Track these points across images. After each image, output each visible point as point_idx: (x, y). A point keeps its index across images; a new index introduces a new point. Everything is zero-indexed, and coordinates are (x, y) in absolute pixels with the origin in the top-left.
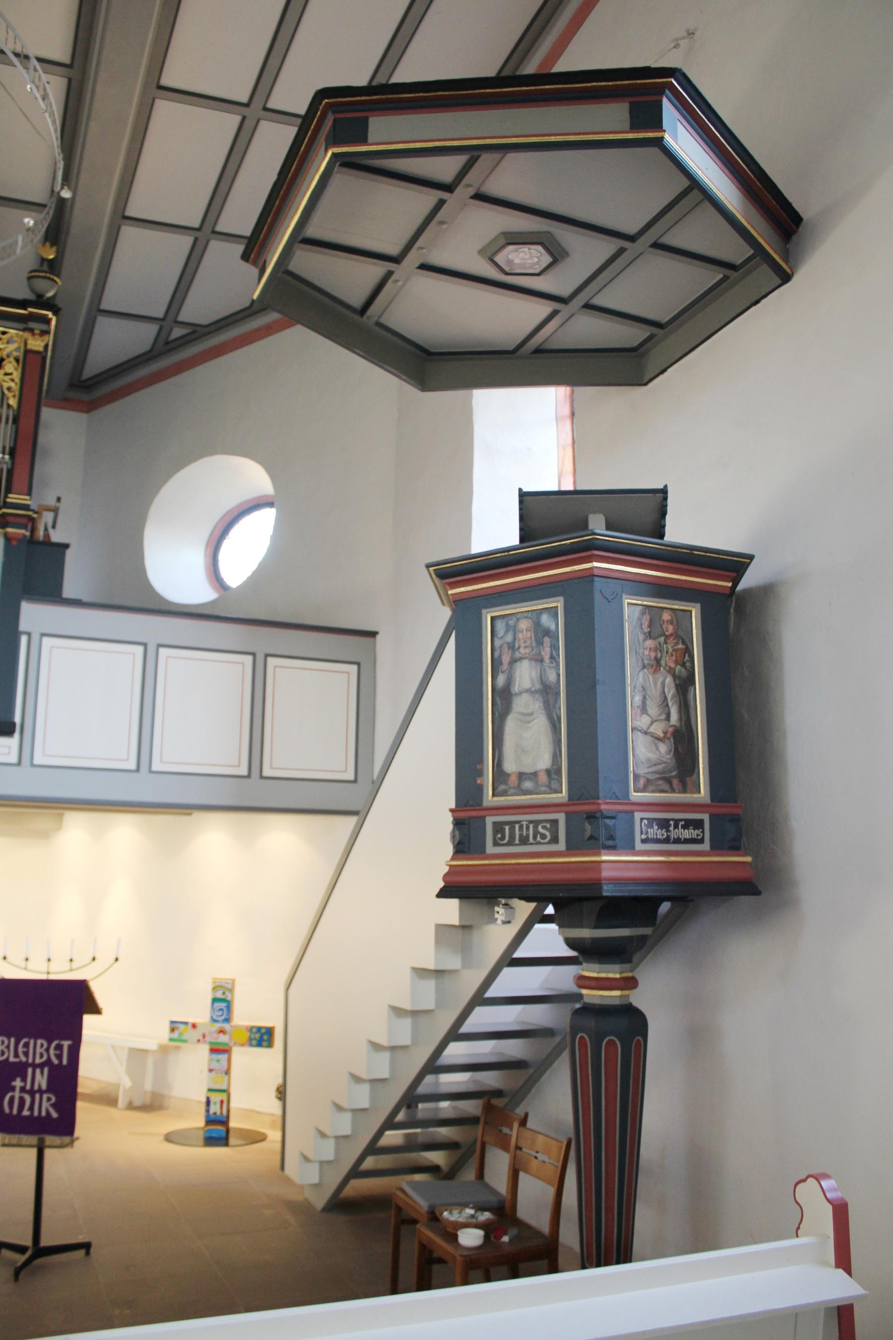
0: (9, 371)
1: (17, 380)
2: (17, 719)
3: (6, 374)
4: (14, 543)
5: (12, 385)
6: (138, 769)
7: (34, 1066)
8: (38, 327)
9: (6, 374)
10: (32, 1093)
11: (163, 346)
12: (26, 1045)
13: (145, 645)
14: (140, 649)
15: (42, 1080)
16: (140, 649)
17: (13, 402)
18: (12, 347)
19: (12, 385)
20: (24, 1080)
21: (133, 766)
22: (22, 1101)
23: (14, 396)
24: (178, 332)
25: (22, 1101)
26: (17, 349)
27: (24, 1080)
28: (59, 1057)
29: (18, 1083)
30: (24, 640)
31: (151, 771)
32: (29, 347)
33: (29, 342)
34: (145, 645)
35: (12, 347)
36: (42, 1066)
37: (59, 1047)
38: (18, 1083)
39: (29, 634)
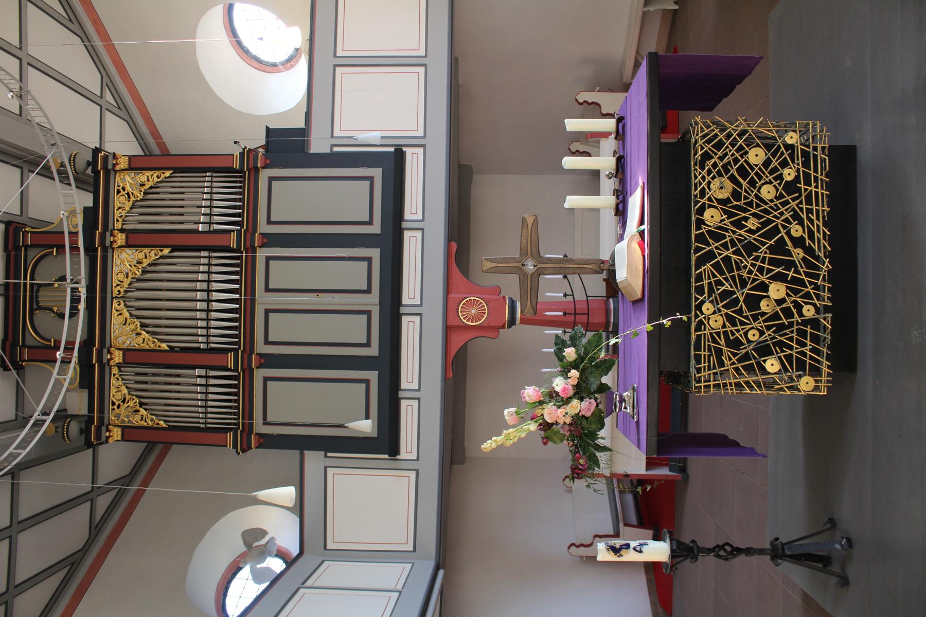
0: (146, 179)
1: (152, 173)
2: (392, 149)
5: (155, 175)
6: (425, 65)
11: (121, 109)
13: (335, 66)
14: (339, 70)
16: (339, 70)
17: (168, 173)
18: (128, 178)
19: (155, 175)
24: (109, 97)
30: (336, 149)
32: (126, 166)
33: (122, 167)
34: (335, 66)
39: (333, 146)
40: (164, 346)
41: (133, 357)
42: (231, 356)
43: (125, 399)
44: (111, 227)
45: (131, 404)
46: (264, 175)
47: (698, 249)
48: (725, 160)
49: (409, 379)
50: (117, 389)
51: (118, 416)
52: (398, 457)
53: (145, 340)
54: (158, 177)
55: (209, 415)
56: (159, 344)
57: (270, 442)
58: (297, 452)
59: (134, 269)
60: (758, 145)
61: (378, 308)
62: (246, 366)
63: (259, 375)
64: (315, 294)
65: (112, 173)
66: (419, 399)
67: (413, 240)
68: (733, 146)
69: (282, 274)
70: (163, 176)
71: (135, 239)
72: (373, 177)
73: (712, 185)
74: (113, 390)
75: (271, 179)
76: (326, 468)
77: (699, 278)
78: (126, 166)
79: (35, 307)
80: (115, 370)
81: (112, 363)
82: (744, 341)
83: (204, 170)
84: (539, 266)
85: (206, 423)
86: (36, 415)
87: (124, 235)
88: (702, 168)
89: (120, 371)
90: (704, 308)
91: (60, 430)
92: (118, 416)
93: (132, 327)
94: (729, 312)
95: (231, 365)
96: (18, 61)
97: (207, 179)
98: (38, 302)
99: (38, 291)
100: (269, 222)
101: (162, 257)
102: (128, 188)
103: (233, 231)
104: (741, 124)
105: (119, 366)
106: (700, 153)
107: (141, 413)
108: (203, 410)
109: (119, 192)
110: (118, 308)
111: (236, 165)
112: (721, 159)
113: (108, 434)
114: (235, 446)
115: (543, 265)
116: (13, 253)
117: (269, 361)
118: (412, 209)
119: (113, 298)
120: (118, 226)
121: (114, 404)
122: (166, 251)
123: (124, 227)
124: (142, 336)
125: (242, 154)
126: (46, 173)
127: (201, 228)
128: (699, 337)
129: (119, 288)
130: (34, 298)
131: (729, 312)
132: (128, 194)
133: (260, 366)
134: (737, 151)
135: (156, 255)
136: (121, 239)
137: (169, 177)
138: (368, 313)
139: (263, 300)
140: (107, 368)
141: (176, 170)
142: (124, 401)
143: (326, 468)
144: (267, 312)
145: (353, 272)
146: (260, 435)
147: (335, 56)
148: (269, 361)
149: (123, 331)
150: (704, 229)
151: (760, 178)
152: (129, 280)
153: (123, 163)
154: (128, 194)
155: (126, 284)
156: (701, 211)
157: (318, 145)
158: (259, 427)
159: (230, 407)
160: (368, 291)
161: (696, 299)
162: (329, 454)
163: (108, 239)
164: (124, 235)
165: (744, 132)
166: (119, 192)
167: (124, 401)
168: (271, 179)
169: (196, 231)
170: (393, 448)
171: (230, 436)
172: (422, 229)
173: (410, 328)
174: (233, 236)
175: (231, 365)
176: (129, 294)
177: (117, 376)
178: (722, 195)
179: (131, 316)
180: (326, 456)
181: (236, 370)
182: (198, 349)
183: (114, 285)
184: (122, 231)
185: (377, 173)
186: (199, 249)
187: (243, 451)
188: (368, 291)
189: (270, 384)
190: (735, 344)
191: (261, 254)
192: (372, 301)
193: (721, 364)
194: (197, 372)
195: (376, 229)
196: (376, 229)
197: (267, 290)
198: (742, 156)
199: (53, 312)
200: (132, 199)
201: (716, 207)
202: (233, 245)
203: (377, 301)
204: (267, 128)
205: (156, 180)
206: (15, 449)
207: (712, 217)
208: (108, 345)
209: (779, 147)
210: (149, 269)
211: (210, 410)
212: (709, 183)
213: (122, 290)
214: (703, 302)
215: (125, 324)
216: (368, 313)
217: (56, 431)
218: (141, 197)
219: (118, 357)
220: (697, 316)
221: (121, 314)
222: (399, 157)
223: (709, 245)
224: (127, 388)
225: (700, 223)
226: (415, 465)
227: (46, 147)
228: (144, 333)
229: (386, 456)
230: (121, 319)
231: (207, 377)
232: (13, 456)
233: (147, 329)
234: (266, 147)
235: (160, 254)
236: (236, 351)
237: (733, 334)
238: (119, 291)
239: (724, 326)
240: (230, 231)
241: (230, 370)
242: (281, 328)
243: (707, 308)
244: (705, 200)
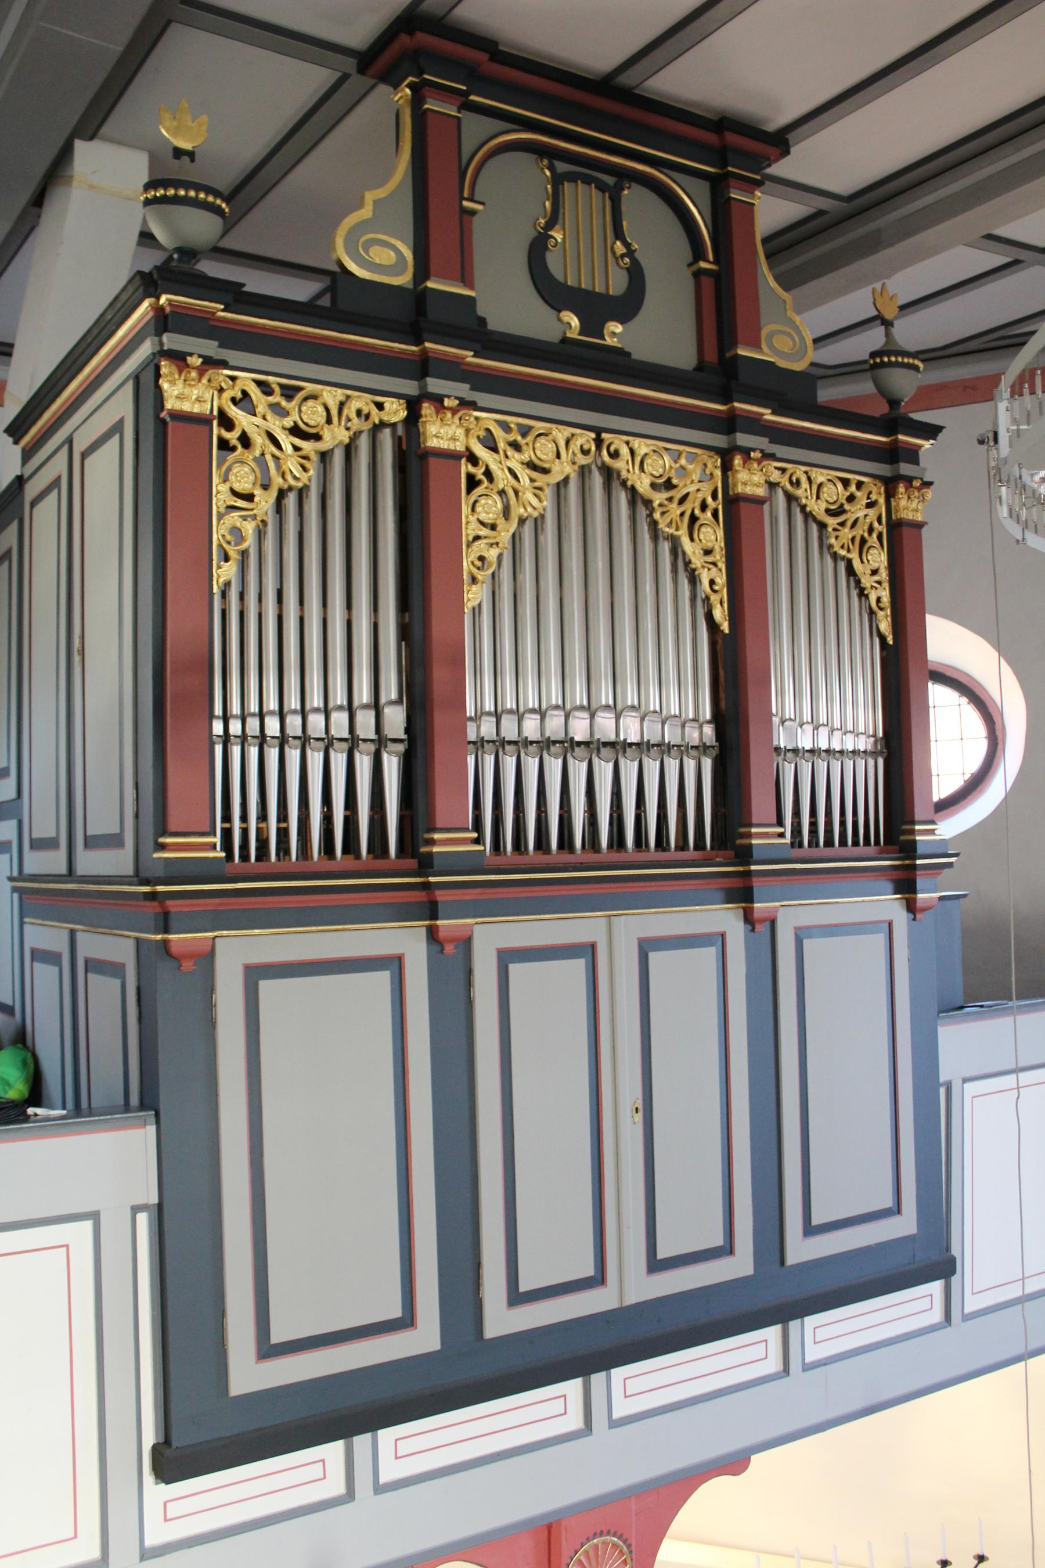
52: (148, 1477)
61: (614, 1304)
66: (350, 1494)
69: (686, 986)
79: (562, 167)
98: (572, 177)
99: (602, 187)
113: (196, 361)
116: (710, 138)
117: (452, 966)
119: (598, 431)
124: (501, 523)
144: (589, 951)
148: (452, 966)
159: (263, 817)
162: (143, 1218)
177: (376, 416)
180: (135, 1210)
183: (636, 442)
189: (383, 978)
199: (551, 224)
200: (832, 522)
203: (632, 1298)
211: (272, 755)
231: (381, 741)
242: (548, 997)
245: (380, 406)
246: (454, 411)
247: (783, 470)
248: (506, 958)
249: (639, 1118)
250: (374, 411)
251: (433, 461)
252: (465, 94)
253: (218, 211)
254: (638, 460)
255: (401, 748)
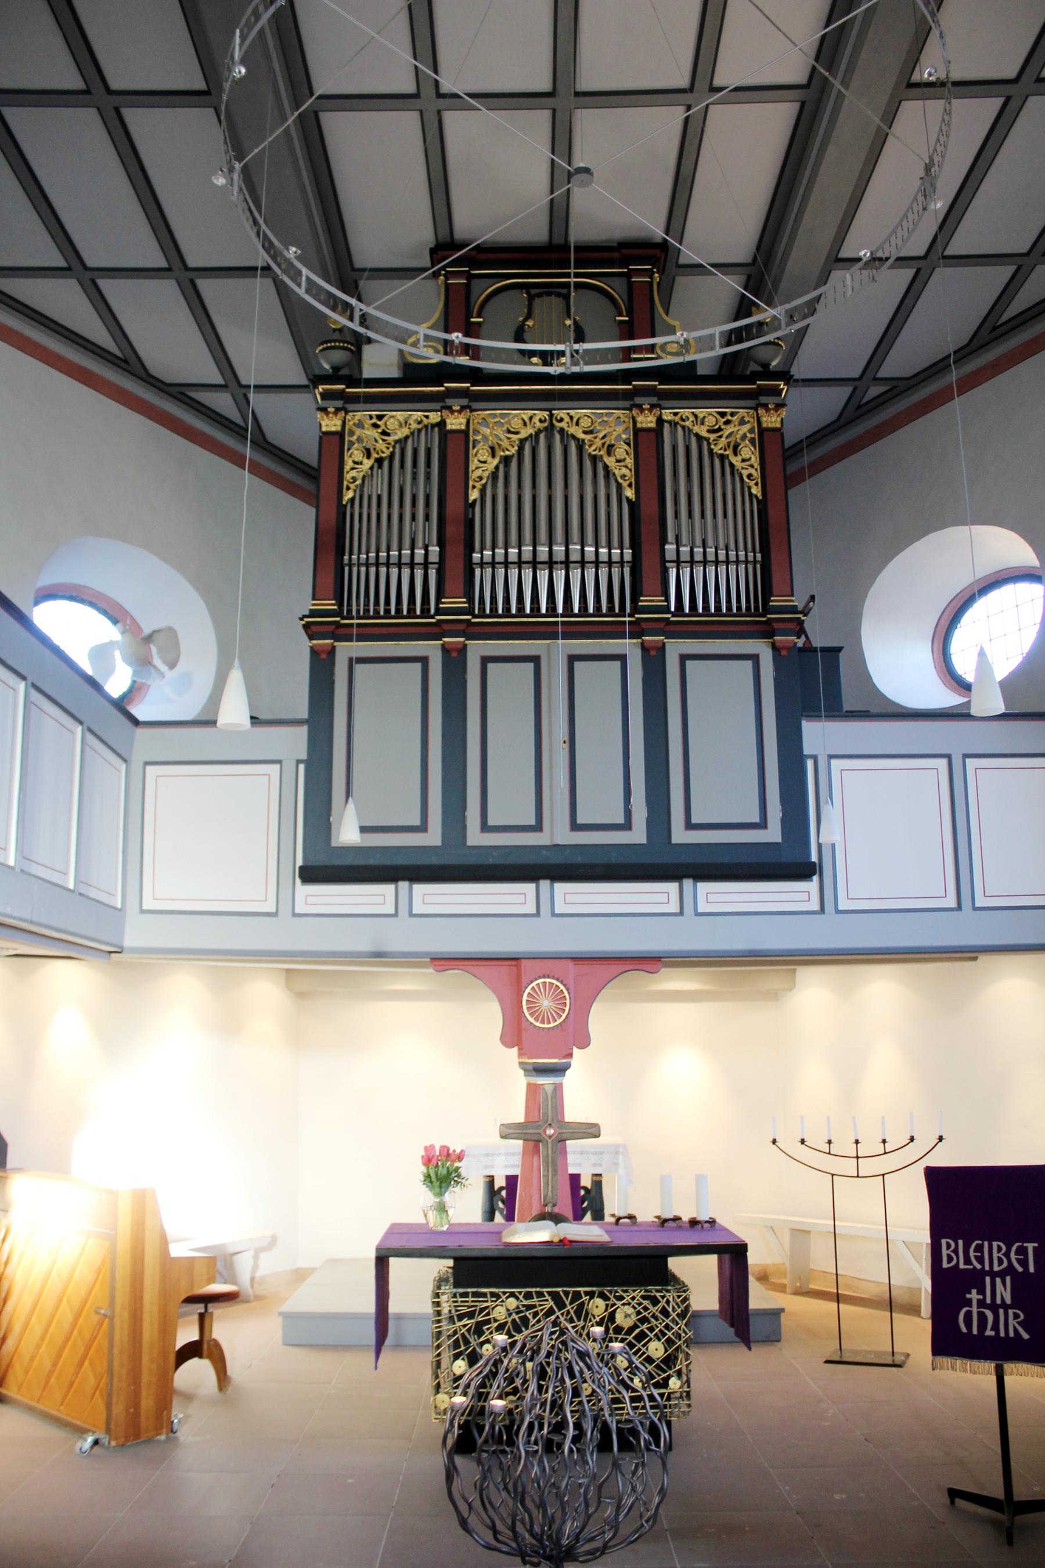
0: (748, 456)
1: (756, 465)
2: (814, 858)
3: (743, 461)
4: (784, 653)
5: (753, 471)
6: (959, 907)
7: (993, 1275)
8: (771, 401)
9: (743, 461)
10: (994, 1308)
12: (979, 1249)
13: (949, 757)
14: (943, 763)
15: (1004, 1292)
16: (943, 763)
18: (745, 428)
19: (753, 471)
20: (982, 1291)
21: (953, 904)
22: (982, 1318)
23: (756, 484)
25: (982, 1318)
26: (751, 431)
27: (982, 1291)
28: (1024, 1263)
29: (974, 1295)
30: (810, 764)
31: (975, 909)
32: (765, 425)
33: (764, 419)
34: (949, 757)
35: (747, 427)
36: (1002, 1274)
37: (1021, 1251)
38: (974, 1295)
40: (474, 495)
41: (454, 447)
42: (461, 603)
43: (388, 435)
44: (664, 403)
45: (381, 445)
46: (761, 648)
47: (567, 1293)
48: (652, 1320)
49: (430, 896)
50: (401, 421)
51: (360, 425)
52: (298, 881)
53: (482, 464)
54: (749, 476)
55: (363, 569)
56: (478, 485)
57: (322, 666)
58: (304, 714)
59: (598, 443)
60: (666, 1351)
61: (547, 842)
62: (445, 627)
63: (431, 649)
64: (566, 738)
65: (752, 403)
67: (663, 898)
68: (667, 1327)
69: (599, 684)
70: (752, 483)
71: (647, 444)
72: (766, 827)
73: (627, 1307)
74: (400, 415)
75: (755, 658)
76: (279, 762)
77: (540, 1295)
78: (765, 425)
79: (533, 291)
80: (434, 417)
81: (445, 413)
82: (482, 1339)
83: (765, 549)
84: (550, 1141)
85: (350, 565)
86: (362, 306)
87: (653, 425)
88: (643, 1297)
89: (433, 426)
90: (512, 1300)
91: (337, 336)
92: (360, 425)
93: (505, 443)
94: (509, 1324)
95: (447, 603)
96: (922, 253)
97: (751, 555)
98: (540, 295)
99: (559, 295)
100: (684, 658)
101: (619, 486)
102: (728, 430)
103: (667, 600)
104: (686, 1334)
105: (442, 424)
106: (658, 1295)
107: (365, 461)
108: (372, 561)
109: (723, 415)
110: (536, 420)
111: (776, 601)
112: (654, 1316)
114: (313, 613)
115: (550, 1146)
116: (616, 255)
117: (454, 663)
118: (714, 895)
119: (550, 410)
120: (667, 415)
121: (380, 418)
122: (630, 493)
123: (666, 425)
124: (490, 459)
125: (794, 610)
126: (743, 308)
127: (670, 548)
128: (484, 1295)
129: (567, 419)
130: (548, 290)
131: (509, 1324)
132: (720, 429)
133: (445, 650)
134: (660, 1330)
135: (623, 476)
136: (647, 420)
137: (750, 494)
138: (538, 827)
139: (556, 651)
140: (438, 406)
141: (763, 504)
142: (385, 433)
143: (279, 762)
144: (536, 660)
145: (606, 800)
146: (332, 651)
147: (966, 756)
148: (454, 663)
149: (499, 430)
150: (585, 1298)
151: (635, 1353)
152: (581, 436)
153: (771, 420)
154: (720, 429)
155: (572, 430)
156: (602, 1296)
157: (817, 735)
158: (345, 650)
159: (377, 603)
160: (575, 827)
161: (520, 1293)
162: (302, 767)
163: (646, 402)
164: (653, 425)
165: (679, 1337)
166: (723, 415)
167: (385, 433)
168: (755, 658)
169: (664, 541)
170: (310, 874)
171: (330, 605)
172: (681, 913)
173: (515, 896)
174: (658, 601)
175: (447, 603)
176: (557, 437)
178: (619, 1318)
179: (522, 442)
180: (299, 762)
181: (438, 611)
182: (472, 550)
183: (572, 412)
184: (660, 421)
185: (773, 834)
186: (635, 545)
187: (306, 627)
188: (575, 827)
190: (478, 1330)
191: (629, 646)
192: (557, 833)
193: (461, 1317)
194: (434, 549)
195: (680, 835)
196: (680, 835)
197: (572, 659)
198: (656, 1335)
199: (525, 320)
200: (712, 437)
201: (606, 1310)
202: (645, 601)
204: (839, 649)
205: (745, 473)
206: (308, 278)
207: (598, 1307)
208: (475, 405)
209: (665, 1371)
210: (600, 466)
212: (629, 1304)
213: (563, 425)
214: (517, 1298)
215: (509, 432)
216: (538, 827)
217: (334, 330)
218: (716, 449)
219: (455, 422)
220: (504, 1293)
221: (525, 424)
222: (801, 869)
223: (571, 1303)
224: (407, 438)
225: (591, 1295)
226: (285, 912)
227: (788, 306)
228: (496, 461)
229: (299, 862)
230: (516, 424)
231: (426, 565)
232: (296, 276)
233: (501, 467)
234: (809, 649)
235: (625, 484)
236: (470, 611)
237: (488, 1329)
238: (562, 420)
239: (496, 1321)
240: (666, 594)
241: (438, 601)
243: (512, 1303)
244: (613, 1300)
245: (427, 417)
246: (460, 412)
247: (675, 414)
248: (485, 660)
249: (566, 746)
250: (424, 419)
251: (449, 435)
252: (468, 272)
253: (347, 349)
254: (575, 420)
255: (436, 566)
